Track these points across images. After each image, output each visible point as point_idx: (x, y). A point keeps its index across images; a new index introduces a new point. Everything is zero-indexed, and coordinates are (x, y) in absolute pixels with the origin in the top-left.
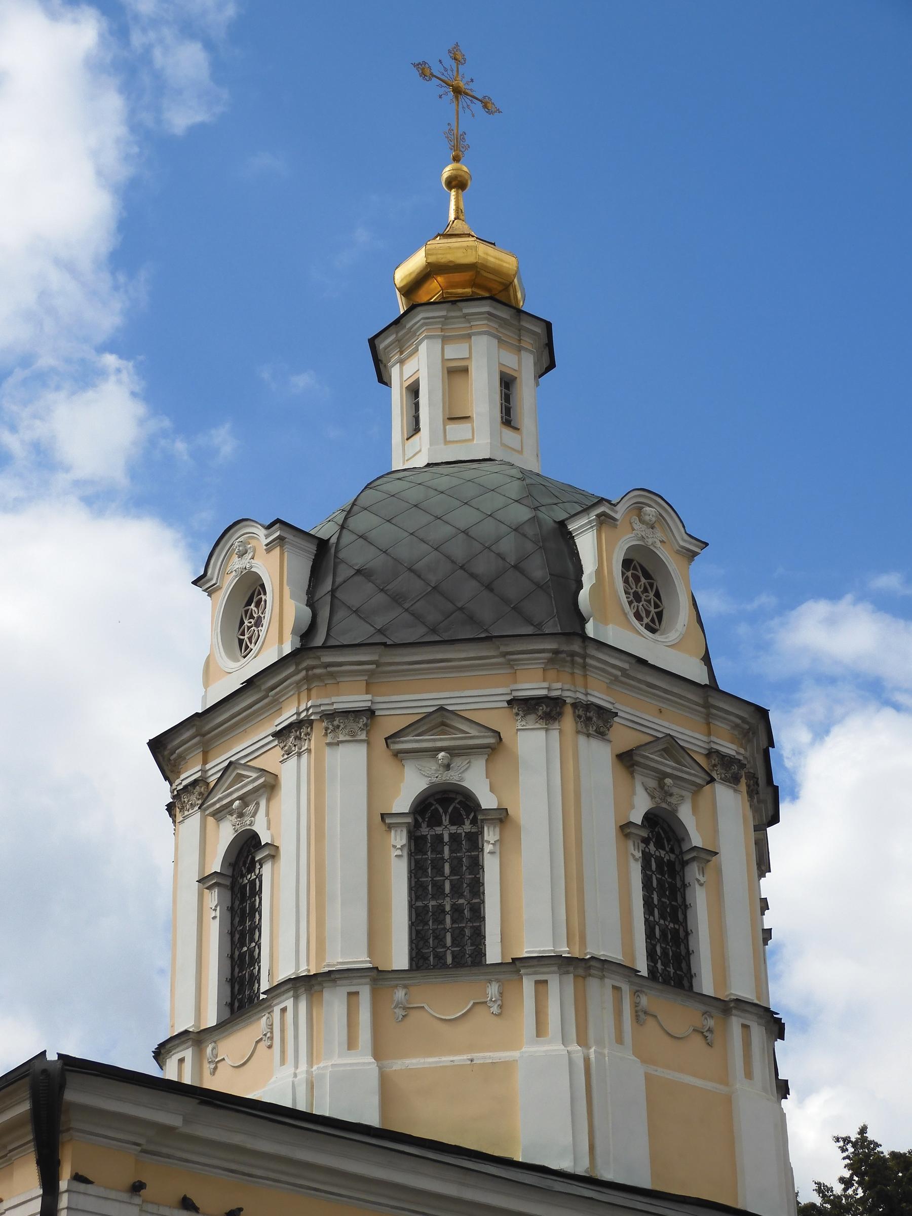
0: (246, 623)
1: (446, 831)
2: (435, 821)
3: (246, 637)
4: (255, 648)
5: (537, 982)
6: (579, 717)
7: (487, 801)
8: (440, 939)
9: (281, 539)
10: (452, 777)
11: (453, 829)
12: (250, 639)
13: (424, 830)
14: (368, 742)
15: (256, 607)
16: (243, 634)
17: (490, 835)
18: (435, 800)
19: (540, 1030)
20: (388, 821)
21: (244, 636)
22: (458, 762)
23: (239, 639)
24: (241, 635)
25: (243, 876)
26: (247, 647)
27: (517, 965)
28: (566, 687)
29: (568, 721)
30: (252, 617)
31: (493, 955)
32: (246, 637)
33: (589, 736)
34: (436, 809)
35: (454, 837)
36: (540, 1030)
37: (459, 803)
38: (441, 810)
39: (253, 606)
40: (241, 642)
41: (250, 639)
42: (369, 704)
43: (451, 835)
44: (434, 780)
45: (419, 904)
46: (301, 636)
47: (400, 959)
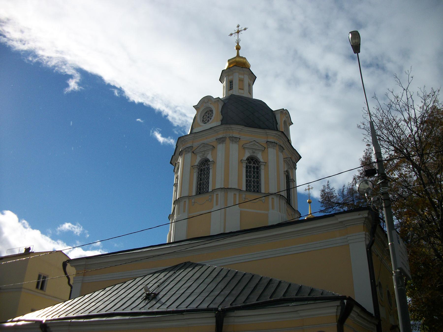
0: (205, 117)
1: (252, 165)
2: (250, 163)
3: (205, 120)
4: (210, 121)
5: (272, 198)
6: (279, 148)
7: (261, 160)
8: (254, 187)
9: (218, 101)
10: (255, 154)
11: (254, 165)
12: (206, 120)
13: (248, 164)
14: (238, 144)
15: (208, 114)
16: (204, 119)
17: (262, 167)
18: (250, 159)
19: (273, 208)
20: (242, 161)
21: (204, 119)
22: (256, 152)
23: (203, 120)
24: (203, 119)
25: (201, 166)
26: (205, 122)
27: (268, 195)
28: (278, 142)
29: (277, 148)
30: (206, 116)
31: (263, 191)
32: (205, 120)
33: (280, 152)
34: (250, 160)
35: (254, 167)
36: (273, 208)
37: (255, 160)
38: (251, 162)
39: (207, 114)
40: (203, 121)
41: (206, 120)
42: (239, 137)
43: (253, 166)
44: (252, 154)
45: (247, 178)
46: (221, 121)
47: (244, 188)
